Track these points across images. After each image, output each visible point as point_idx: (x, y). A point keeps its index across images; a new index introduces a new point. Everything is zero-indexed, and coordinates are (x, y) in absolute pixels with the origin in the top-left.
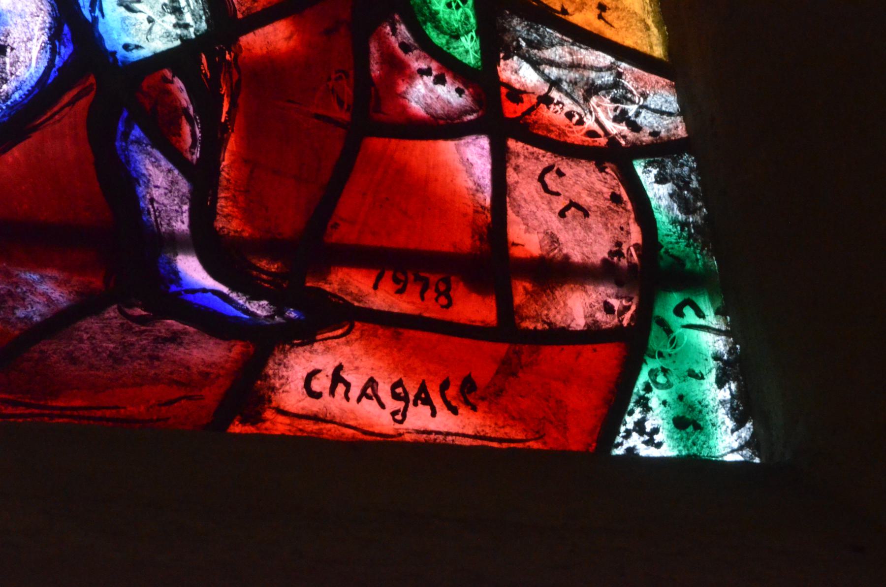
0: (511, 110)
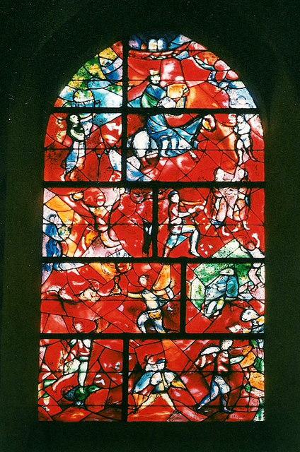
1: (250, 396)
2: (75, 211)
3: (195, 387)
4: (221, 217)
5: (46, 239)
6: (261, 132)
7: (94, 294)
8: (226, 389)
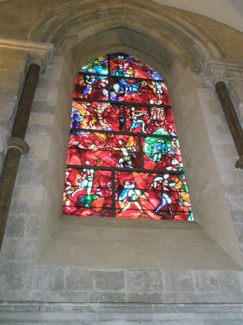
1: (183, 205)
2: (87, 110)
4: (155, 118)
6: (166, 88)
7: (96, 146)
8: (170, 201)
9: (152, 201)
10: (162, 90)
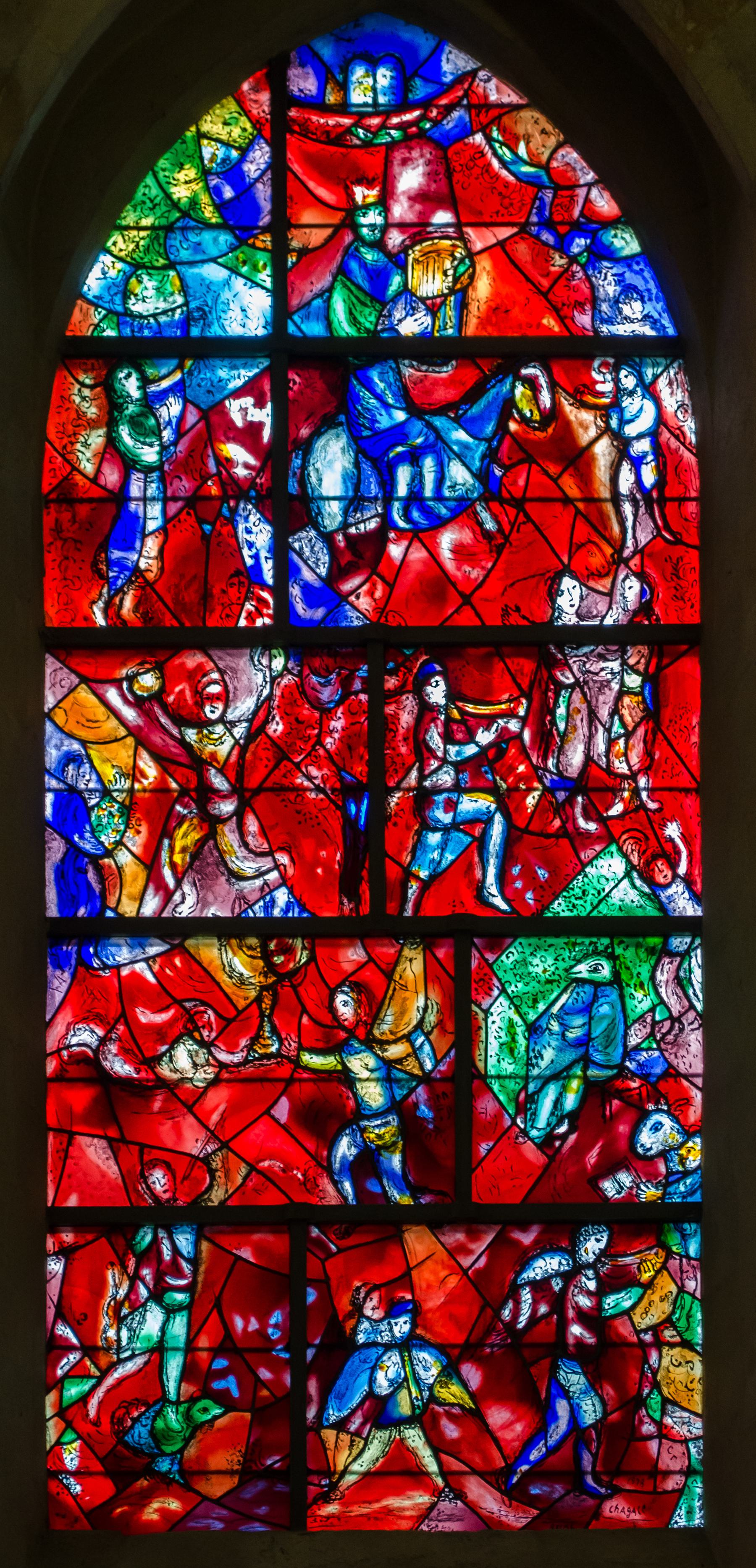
0: (664, 1431)
1: (663, 1433)
3: (502, 1400)
4: (575, 758)
5: (56, 849)
6: (689, 426)
9: (498, 1416)
10: (658, 448)
